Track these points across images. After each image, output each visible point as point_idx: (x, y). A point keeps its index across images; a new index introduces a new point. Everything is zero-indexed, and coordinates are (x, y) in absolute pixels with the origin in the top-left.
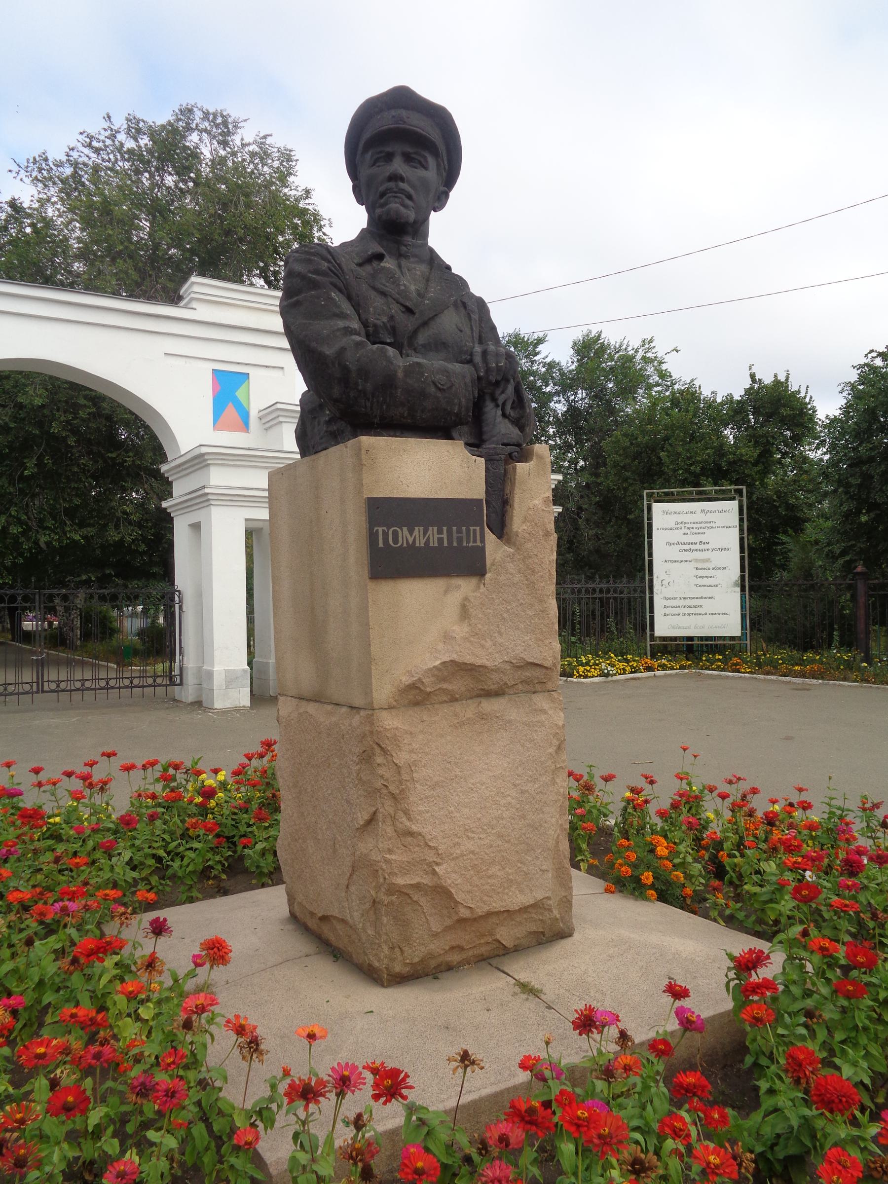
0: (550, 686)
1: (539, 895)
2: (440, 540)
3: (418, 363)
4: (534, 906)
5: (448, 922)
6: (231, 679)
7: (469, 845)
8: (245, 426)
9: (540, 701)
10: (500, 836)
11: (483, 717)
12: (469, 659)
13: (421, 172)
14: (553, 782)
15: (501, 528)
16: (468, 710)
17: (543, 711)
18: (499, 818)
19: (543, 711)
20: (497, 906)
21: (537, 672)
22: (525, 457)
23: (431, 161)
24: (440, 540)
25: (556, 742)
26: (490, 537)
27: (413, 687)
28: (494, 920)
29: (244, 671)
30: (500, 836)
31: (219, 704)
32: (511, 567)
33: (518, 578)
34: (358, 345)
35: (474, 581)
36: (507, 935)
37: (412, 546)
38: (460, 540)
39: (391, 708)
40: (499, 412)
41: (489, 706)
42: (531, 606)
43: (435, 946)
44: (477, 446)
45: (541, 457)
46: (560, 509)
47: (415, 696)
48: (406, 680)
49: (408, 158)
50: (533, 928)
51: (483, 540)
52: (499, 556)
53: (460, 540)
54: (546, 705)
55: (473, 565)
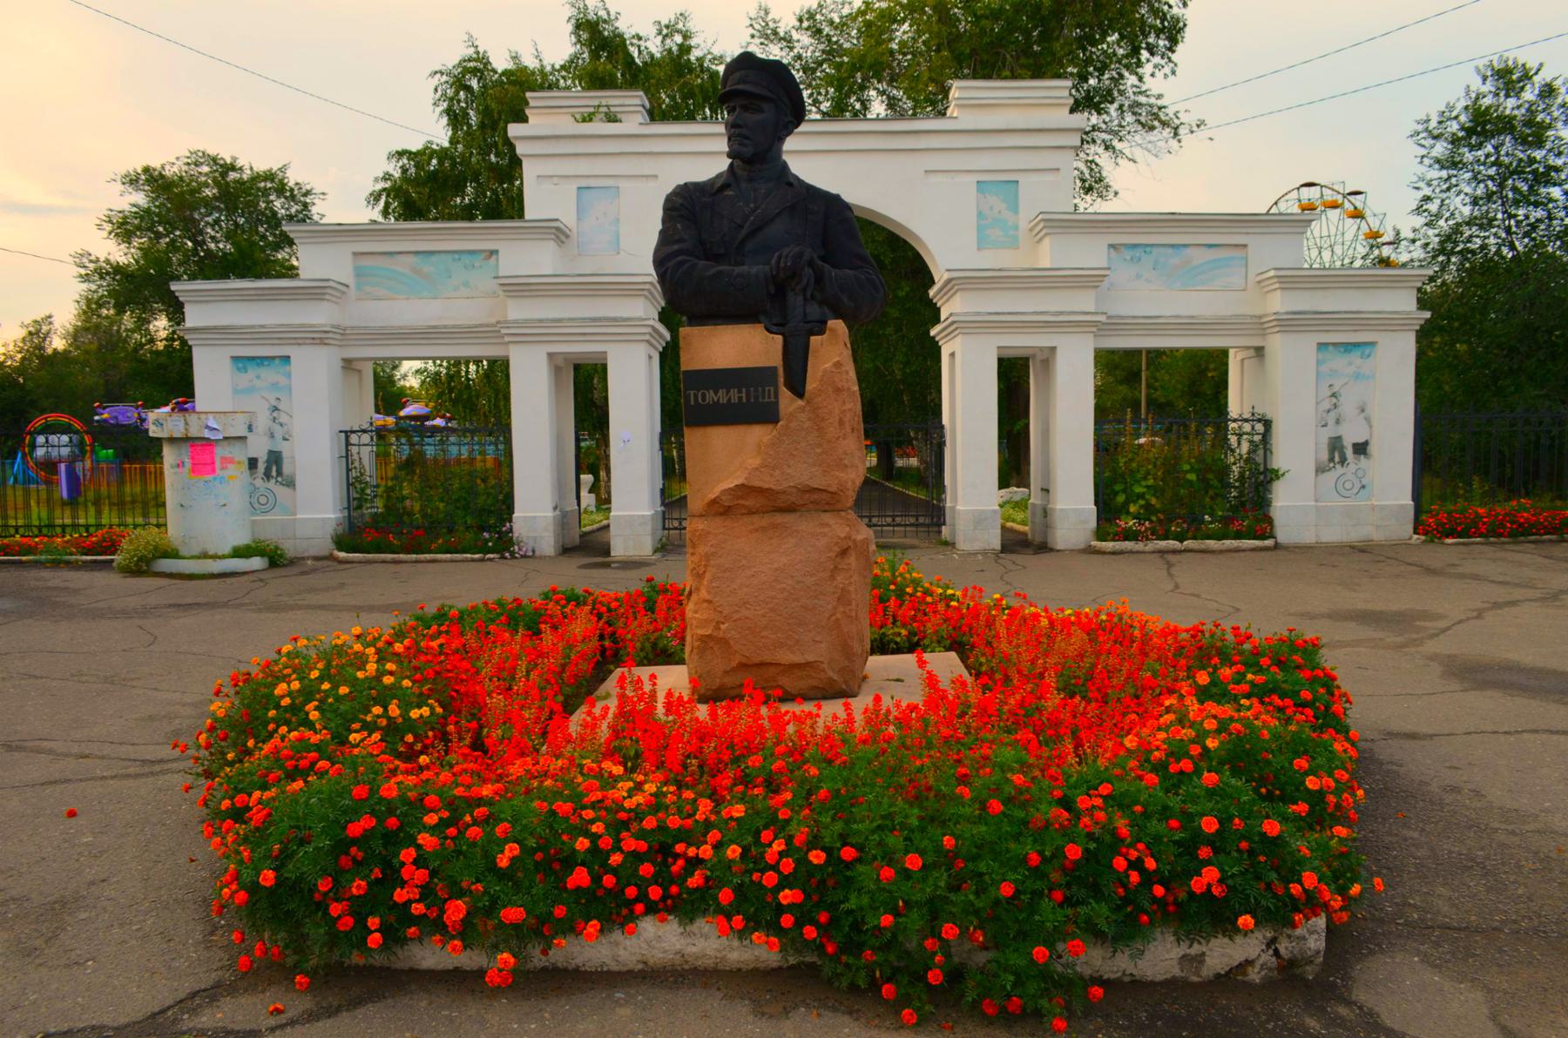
0: (839, 506)
1: (811, 658)
2: (740, 398)
3: (721, 272)
4: (808, 664)
5: (734, 664)
6: (979, 520)
7: (745, 613)
8: (1013, 244)
9: (827, 518)
10: (772, 610)
11: (775, 526)
12: (757, 484)
13: (758, 117)
14: (832, 577)
15: (798, 390)
16: (764, 521)
17: (828, 525)
18: (774, 598)
19: (828, 525)
20: (767, 658)
21: (824, 496)
22: (821, 332)
23: (765, 106)
24: (740, 398)
25: (837, 549)
26: (785, 393)
27: (714, 502)
28: (772, 670)
29: (994, 511)
30: (772, 610)
31: (963, 545)
32: (803, 416)
33: (807, 424)
34: (681, 264)
35: (770, 427)
36: (789, 683)
37: (716, 404)
38: (756, 398)
39: (701, 516)
40: (800, 298)
41: (779, 518)
42: (820, 445)
43: (730, 681)
44: (782, 325)
45: (832, 330)
46: (1428, 315)
47: (721, 509)
48: (712, 496)
49: (745, 108)
50: (815, 683)
51: (776, 396)
52: (791, 409)
53: (756, 398)
54: (832, 522)
55: (767, 415)
